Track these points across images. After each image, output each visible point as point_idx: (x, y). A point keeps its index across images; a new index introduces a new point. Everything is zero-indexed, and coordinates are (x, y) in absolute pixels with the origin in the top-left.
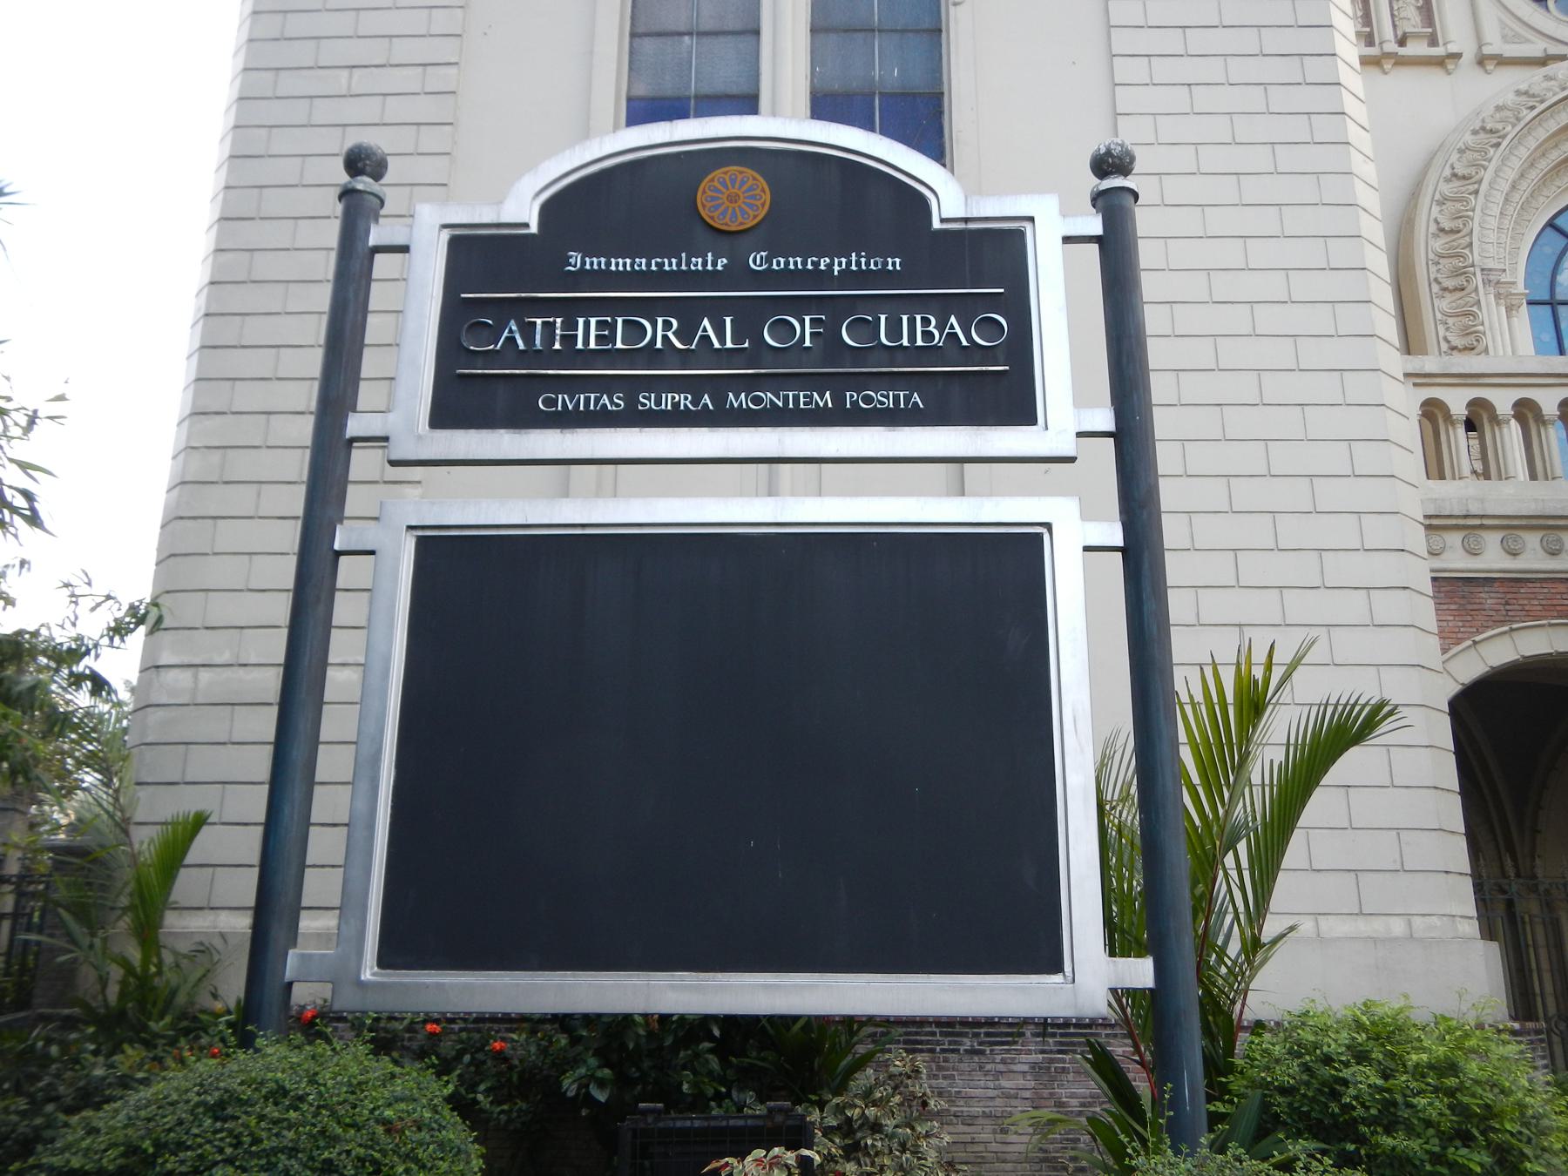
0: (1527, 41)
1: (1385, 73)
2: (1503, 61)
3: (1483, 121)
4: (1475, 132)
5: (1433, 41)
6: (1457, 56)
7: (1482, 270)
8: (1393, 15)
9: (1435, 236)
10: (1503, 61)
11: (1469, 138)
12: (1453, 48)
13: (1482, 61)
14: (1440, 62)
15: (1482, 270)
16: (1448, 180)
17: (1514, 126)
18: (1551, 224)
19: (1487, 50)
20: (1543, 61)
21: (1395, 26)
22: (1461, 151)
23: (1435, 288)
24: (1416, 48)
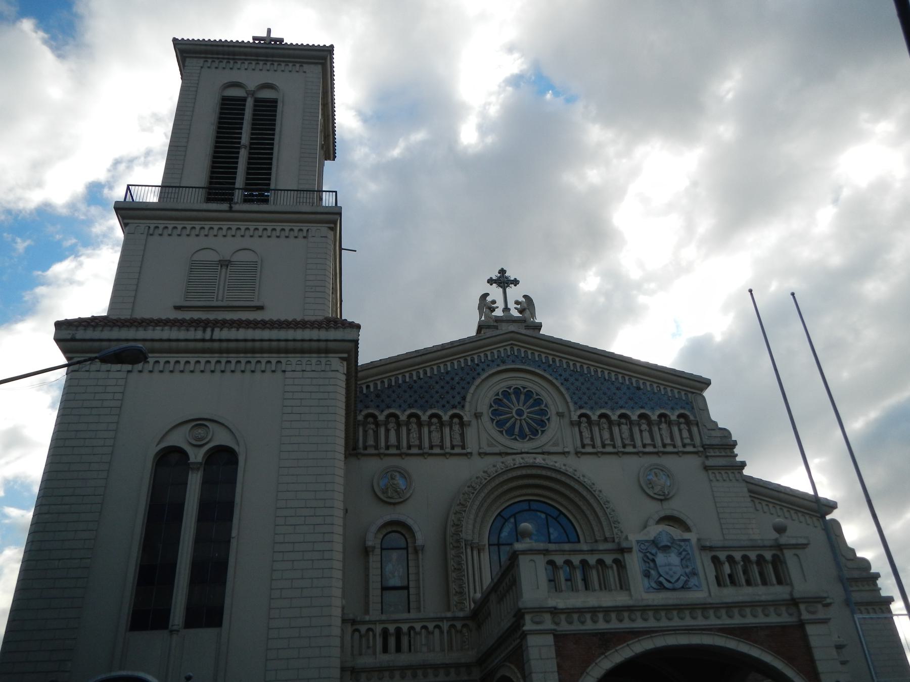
0: (495, 446)
1: (447, 458)
2: (486, 454)
3: (472, 483)
4: (469, 487)
5: (463, 447)
6: (471, 454)
7: (465, 540)
8: (451, 437)
9: (453, 526)
10: (486, 454)
11: (466, 489)
12: (469, 450)
13: (480, 454)
14: (466, 455)
15: (465, 540)
16: (458, 505)
17: (479, 486)
18: (499, 514)
19: (481, 451)
20: (500, 454)
21: (451, 441)
22: (464, 494)
23: (451, 545)
24: (457, 450)
